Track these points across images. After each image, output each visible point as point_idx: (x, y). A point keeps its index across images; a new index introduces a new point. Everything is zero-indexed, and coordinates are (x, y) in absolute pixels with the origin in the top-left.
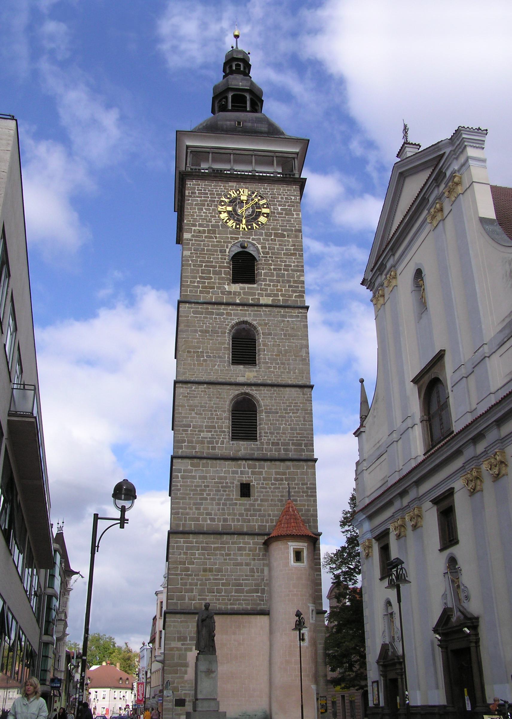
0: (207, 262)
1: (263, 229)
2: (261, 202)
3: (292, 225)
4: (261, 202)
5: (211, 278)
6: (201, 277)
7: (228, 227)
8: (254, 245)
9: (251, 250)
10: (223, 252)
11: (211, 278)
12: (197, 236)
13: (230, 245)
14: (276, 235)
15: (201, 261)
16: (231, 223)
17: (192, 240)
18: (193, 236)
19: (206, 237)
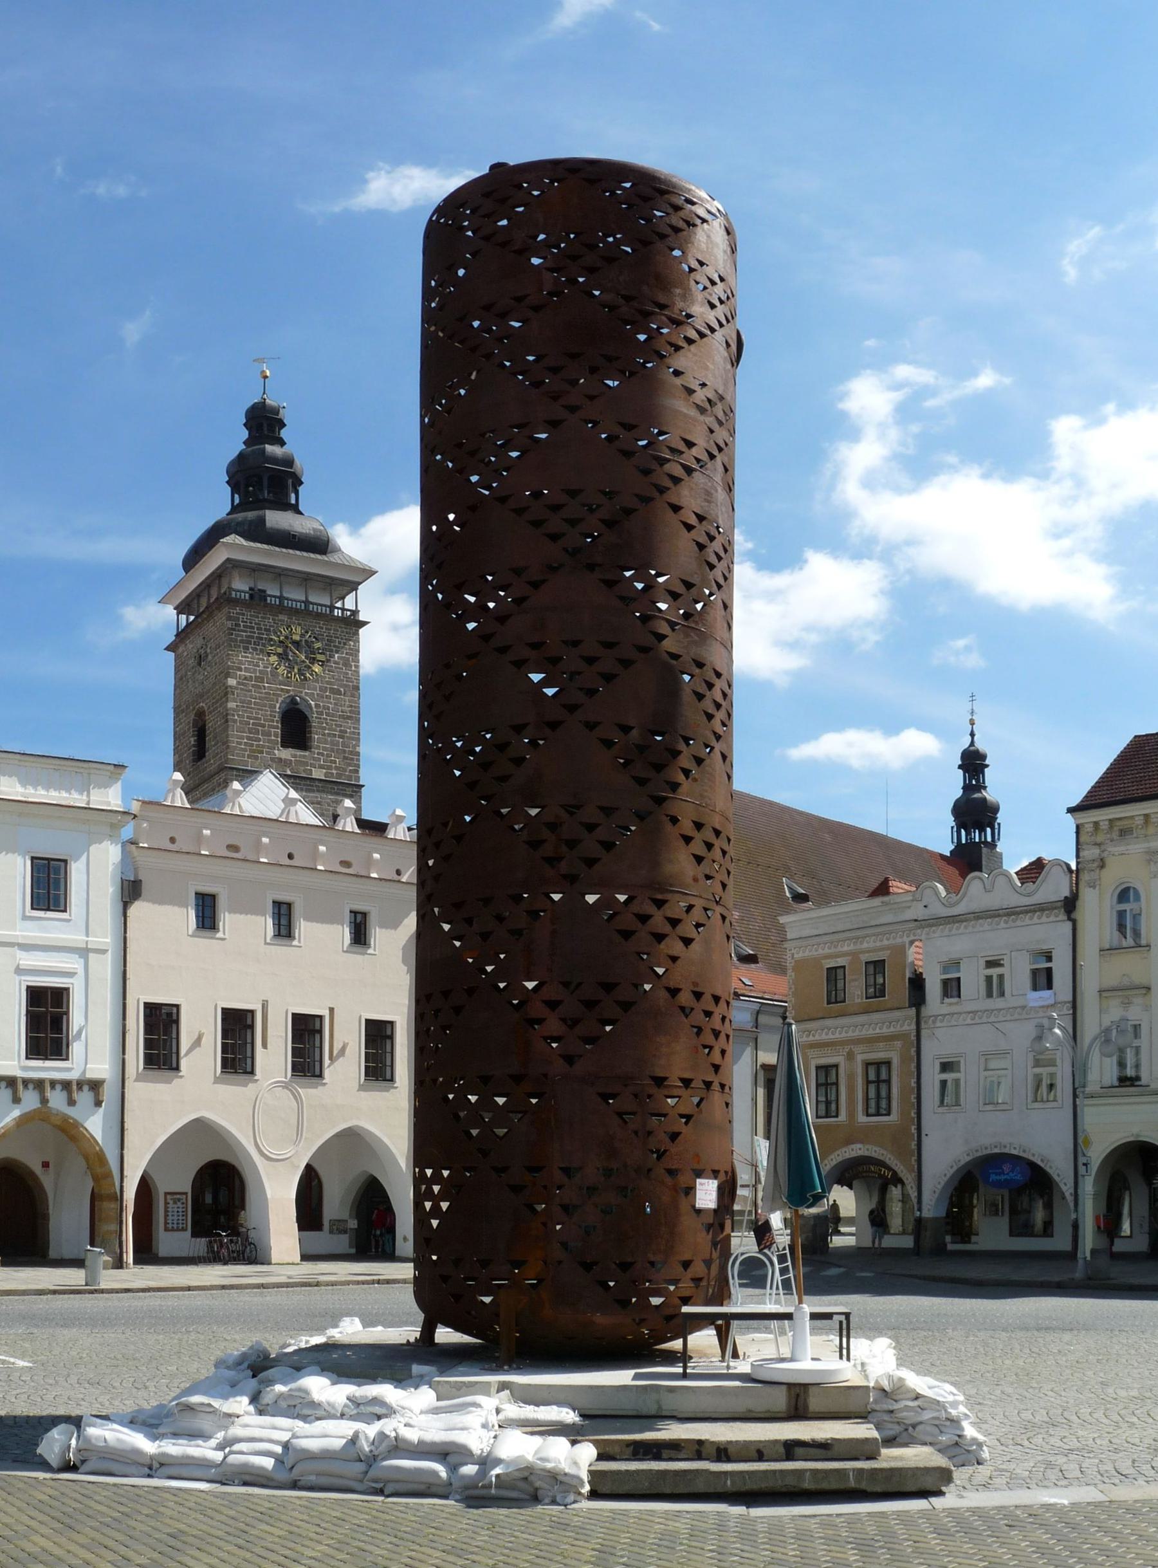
0: (256, 718)
1: (317, 681)
2: (318, 645)
3: (349, 680)
4: (318, 645)
5: (259, 740)
6: (249, 738)
7: (278, 674)
8: (307, 701)
9: (302, 707)
10: (273, 707)
11: (259, 740)
12: (243, 684)
13: (280, 699)
14: (333, 691)
15: (248, 717)
16: (282, 670)
17: (236, 688)
18: (238, 683)
19: (253, 686)
